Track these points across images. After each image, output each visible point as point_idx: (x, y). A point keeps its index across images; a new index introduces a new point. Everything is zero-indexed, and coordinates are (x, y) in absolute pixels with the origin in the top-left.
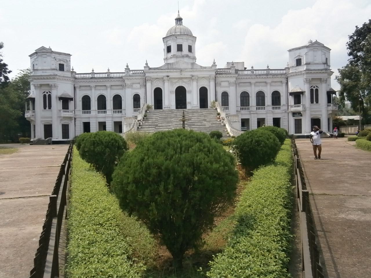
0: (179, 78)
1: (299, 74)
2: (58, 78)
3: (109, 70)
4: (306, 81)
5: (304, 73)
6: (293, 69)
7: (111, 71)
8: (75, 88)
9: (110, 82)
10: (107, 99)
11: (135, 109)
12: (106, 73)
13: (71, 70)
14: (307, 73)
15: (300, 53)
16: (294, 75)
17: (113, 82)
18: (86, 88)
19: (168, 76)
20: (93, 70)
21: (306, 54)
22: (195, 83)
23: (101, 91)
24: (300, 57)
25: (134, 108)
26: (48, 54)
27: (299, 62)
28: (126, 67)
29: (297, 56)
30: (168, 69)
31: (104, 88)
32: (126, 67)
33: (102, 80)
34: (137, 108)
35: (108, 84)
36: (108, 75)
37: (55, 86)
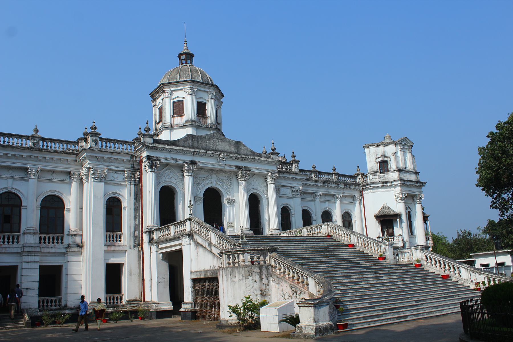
0: (213, 170)
1: (387, 186)
4: (401, 198)
5: (396, 185)
6: (376, 177)
9: (40, 161)
10: (24, 204)
11: (108, 233)
12: (28, 138)
14: (402, 185)
15: (384, 152)
16: (378, 187)
17: (48, 161)
19: (193, 163)
21: (395, 154)
22: (243, 185)
23: (10, 181)
24: (386, 159)
25: (107, 231)
27: (384, 166)
29: (379, 156)
30: (193, 147)
33: (18, 154)
34: (113, 231)
35: (33, 166)
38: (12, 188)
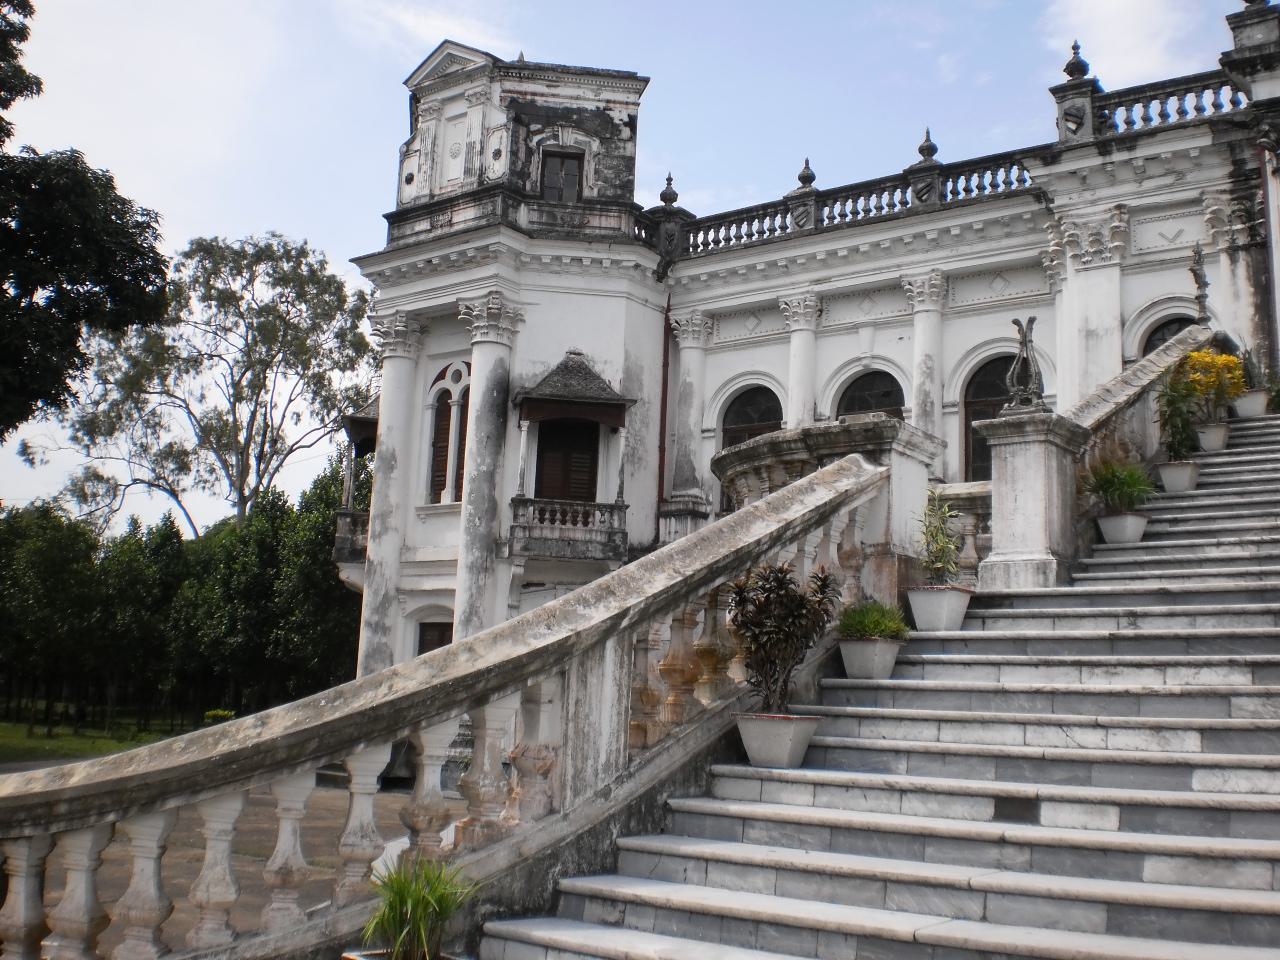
2: (518, 254)
3: (928, 150)
7: (943, 158)
8: (670, 334)
9: (936, 244)
13: (647, 197)
18: (751, 322)
20: (807, 178)
23: (865, 333)
26: (468, 88)
28: (1065, 79)
31: (885, 309)
32: (1065, 79)
35: (920, 267)
36: (918, 195)
37: (502, 318)
38: (873, 357)
